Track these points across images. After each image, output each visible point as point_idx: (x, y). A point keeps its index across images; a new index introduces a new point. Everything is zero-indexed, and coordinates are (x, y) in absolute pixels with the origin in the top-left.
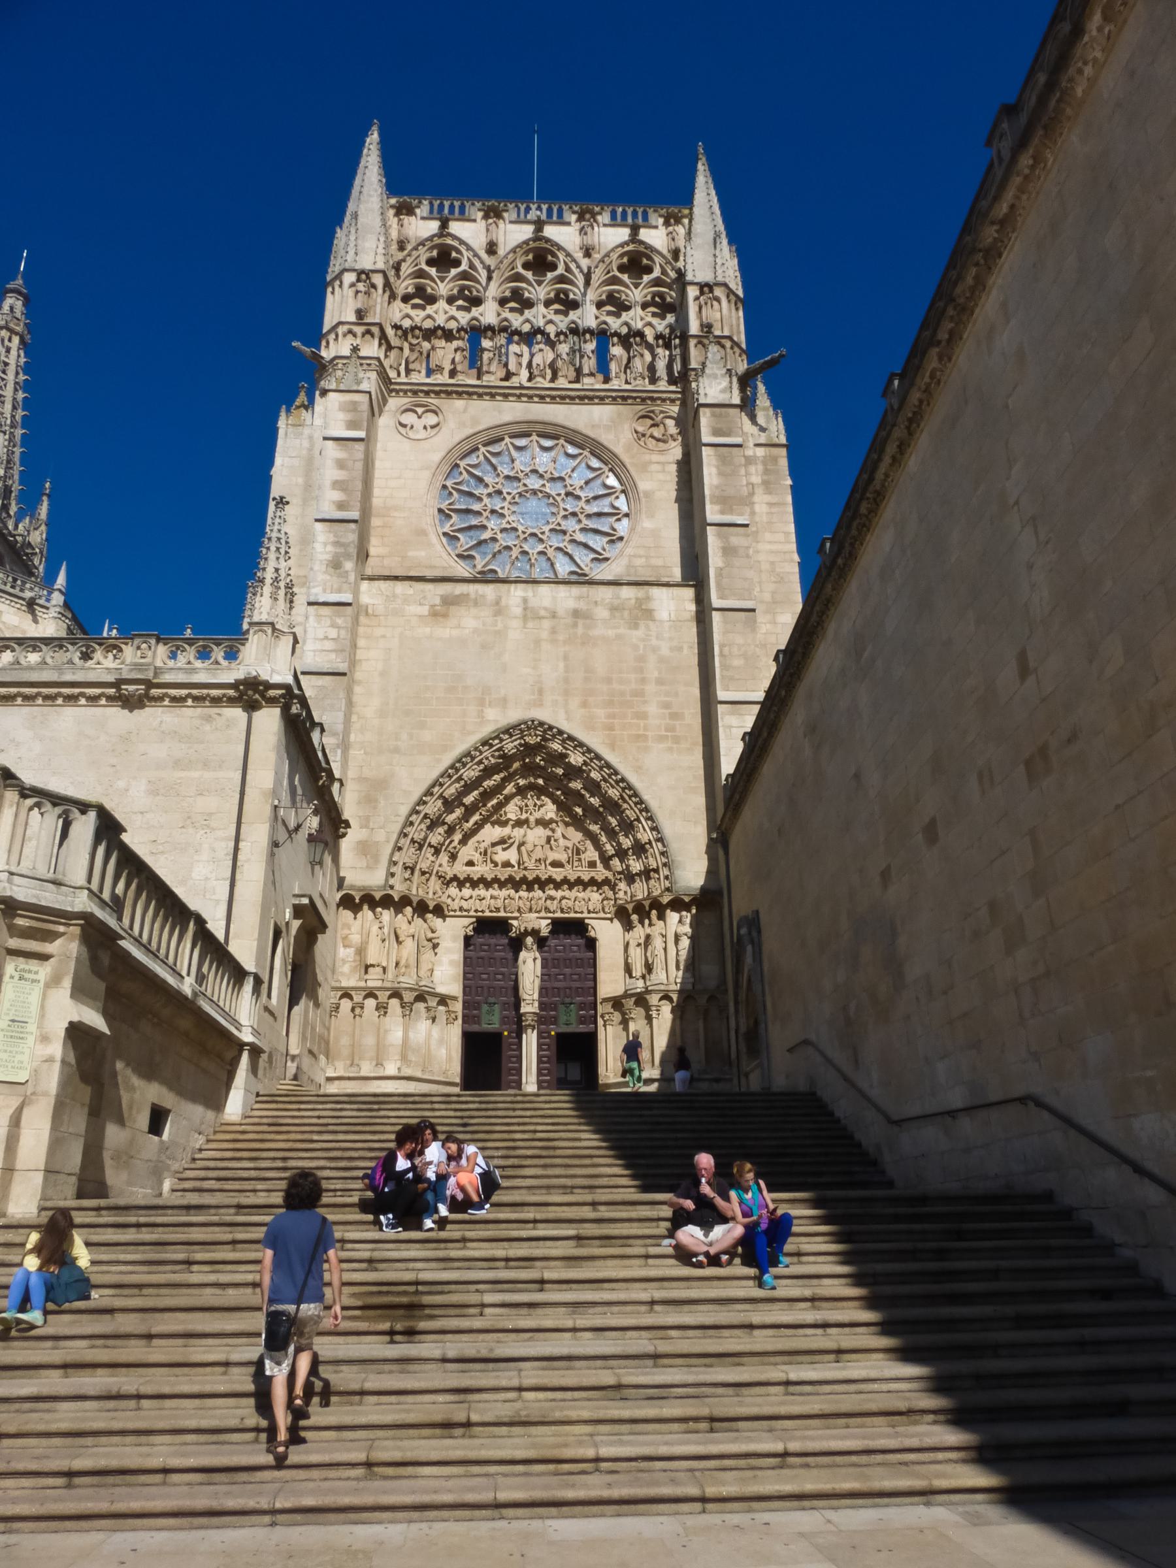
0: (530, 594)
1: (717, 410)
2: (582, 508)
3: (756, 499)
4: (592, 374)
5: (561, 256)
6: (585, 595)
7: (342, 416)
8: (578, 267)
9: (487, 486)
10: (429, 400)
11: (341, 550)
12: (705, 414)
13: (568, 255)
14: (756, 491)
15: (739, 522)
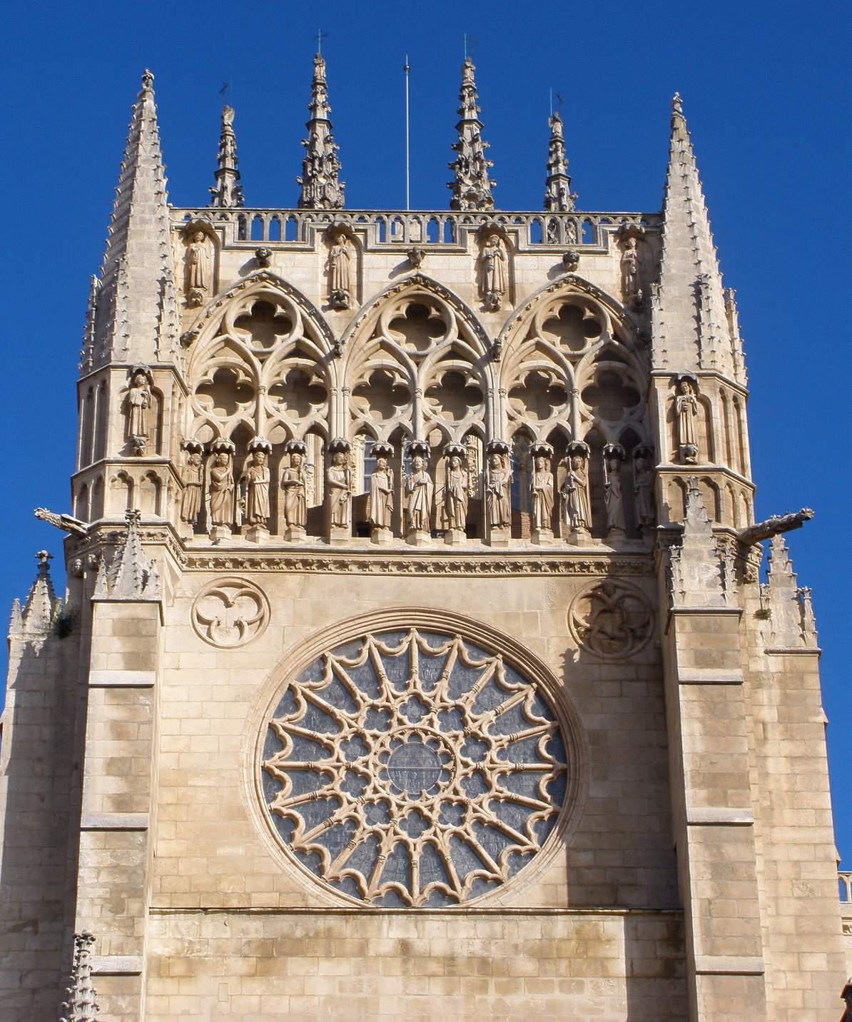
0: (412, 935)
1: (703, 619)
2: (492, 762)
3: (770, 749)
4: (502, 524)
5: (451, 309)
6: (499, 935)
7: (117, 645)
8: (480, 331)
9: (338, 725)
10: (246, 576)
11: (119, 880)
12: (682, 627)
13: (466, 311)
14: (769, 735)
15: (737, 820)
